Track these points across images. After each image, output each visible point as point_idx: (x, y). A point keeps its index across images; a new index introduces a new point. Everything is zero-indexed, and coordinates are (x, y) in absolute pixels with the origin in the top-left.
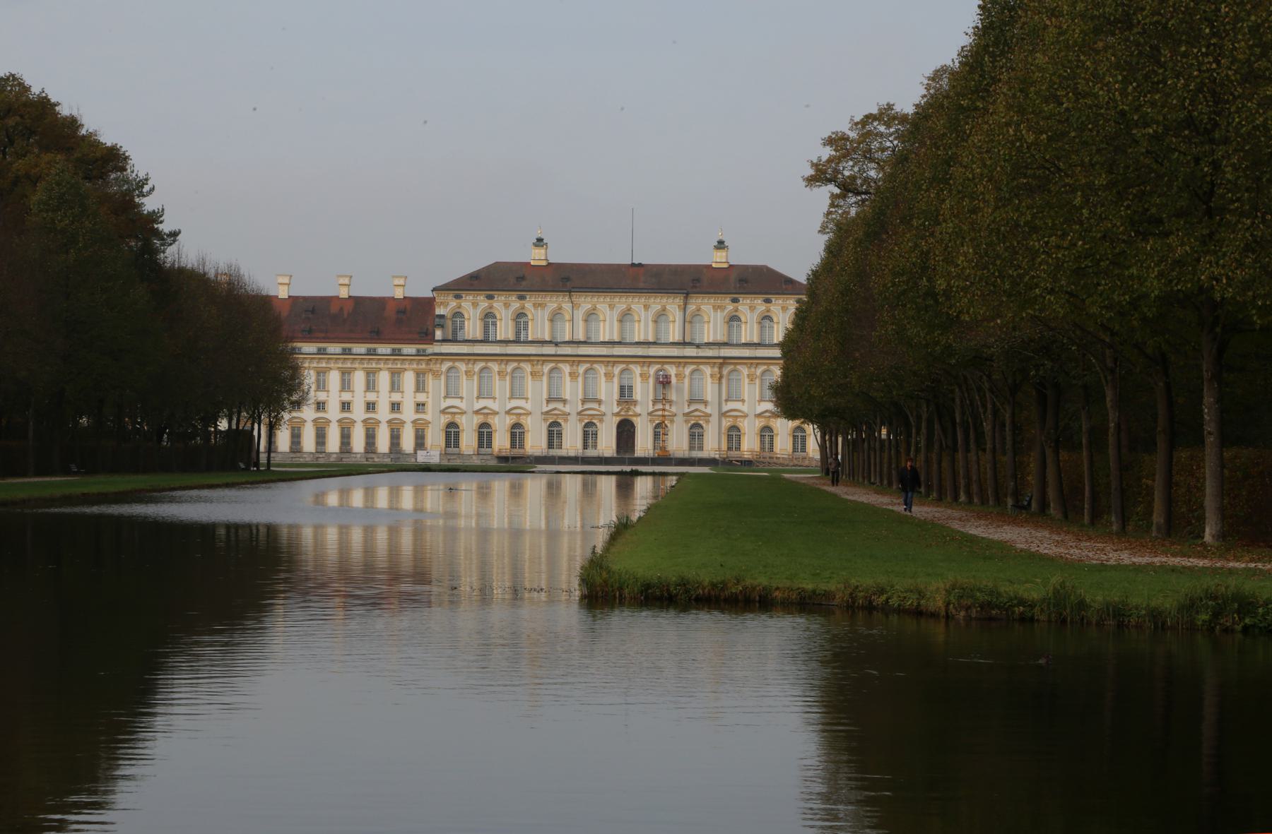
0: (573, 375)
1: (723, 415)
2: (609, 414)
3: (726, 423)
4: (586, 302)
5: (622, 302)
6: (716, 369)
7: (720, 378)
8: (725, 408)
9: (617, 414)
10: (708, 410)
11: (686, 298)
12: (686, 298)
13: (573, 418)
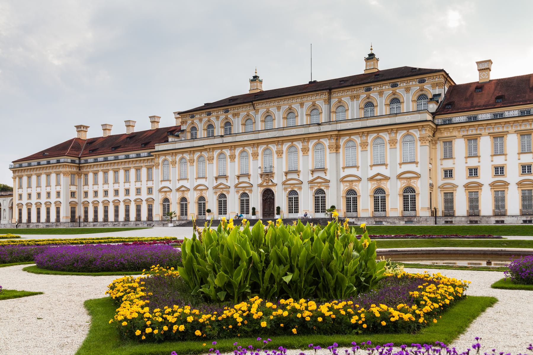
0: (232, 157)
1: (342, 180)
2: (255, 188)
3: (344, 188)
4: (262, 108)
5: (285, 104)
6: (333, 141)
7: (337, 147)
8: (343, 174)
9: (260, 185)
10: (327, 178)
11: (330, 93)
12: (330, 93)
13: (232, 190)
